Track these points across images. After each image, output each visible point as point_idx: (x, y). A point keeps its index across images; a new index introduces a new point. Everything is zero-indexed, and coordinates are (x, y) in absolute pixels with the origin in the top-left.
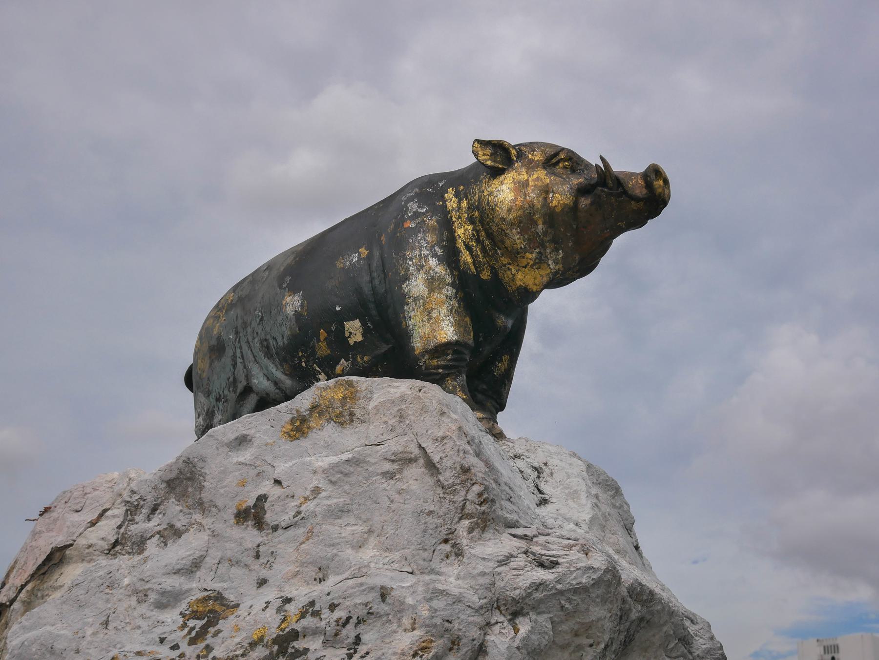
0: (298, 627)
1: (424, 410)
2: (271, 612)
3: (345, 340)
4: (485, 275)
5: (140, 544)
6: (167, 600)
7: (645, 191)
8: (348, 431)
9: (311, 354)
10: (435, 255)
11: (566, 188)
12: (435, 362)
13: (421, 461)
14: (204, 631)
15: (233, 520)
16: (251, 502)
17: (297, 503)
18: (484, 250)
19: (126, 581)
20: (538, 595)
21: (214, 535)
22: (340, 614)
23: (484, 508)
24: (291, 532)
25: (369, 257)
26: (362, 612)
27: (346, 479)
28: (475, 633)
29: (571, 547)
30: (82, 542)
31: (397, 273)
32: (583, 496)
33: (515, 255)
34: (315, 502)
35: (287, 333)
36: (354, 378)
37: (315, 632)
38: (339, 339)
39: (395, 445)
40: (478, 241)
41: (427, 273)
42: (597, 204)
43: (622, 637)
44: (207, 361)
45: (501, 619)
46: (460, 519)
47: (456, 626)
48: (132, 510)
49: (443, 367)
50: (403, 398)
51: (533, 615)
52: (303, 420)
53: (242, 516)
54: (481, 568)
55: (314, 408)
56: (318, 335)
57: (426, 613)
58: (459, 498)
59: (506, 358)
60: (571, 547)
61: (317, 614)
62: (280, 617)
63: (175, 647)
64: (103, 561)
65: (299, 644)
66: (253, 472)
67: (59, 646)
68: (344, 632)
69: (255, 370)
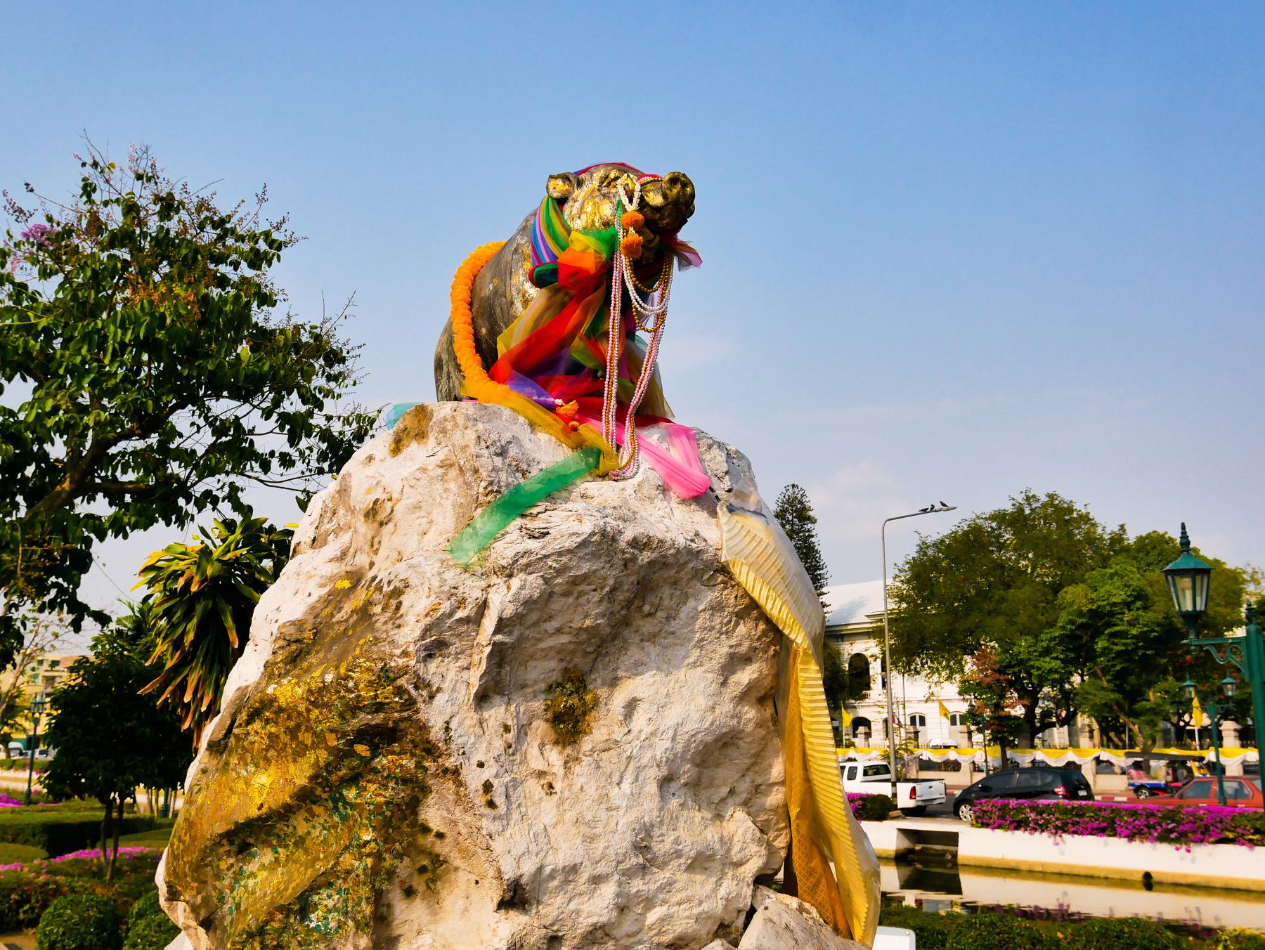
20: (524, 561)
23: (490, 498)
27: (419, 483)
28: (477, 593)
46: (476, 508)
47: (461, 591)
51: (522, 576)
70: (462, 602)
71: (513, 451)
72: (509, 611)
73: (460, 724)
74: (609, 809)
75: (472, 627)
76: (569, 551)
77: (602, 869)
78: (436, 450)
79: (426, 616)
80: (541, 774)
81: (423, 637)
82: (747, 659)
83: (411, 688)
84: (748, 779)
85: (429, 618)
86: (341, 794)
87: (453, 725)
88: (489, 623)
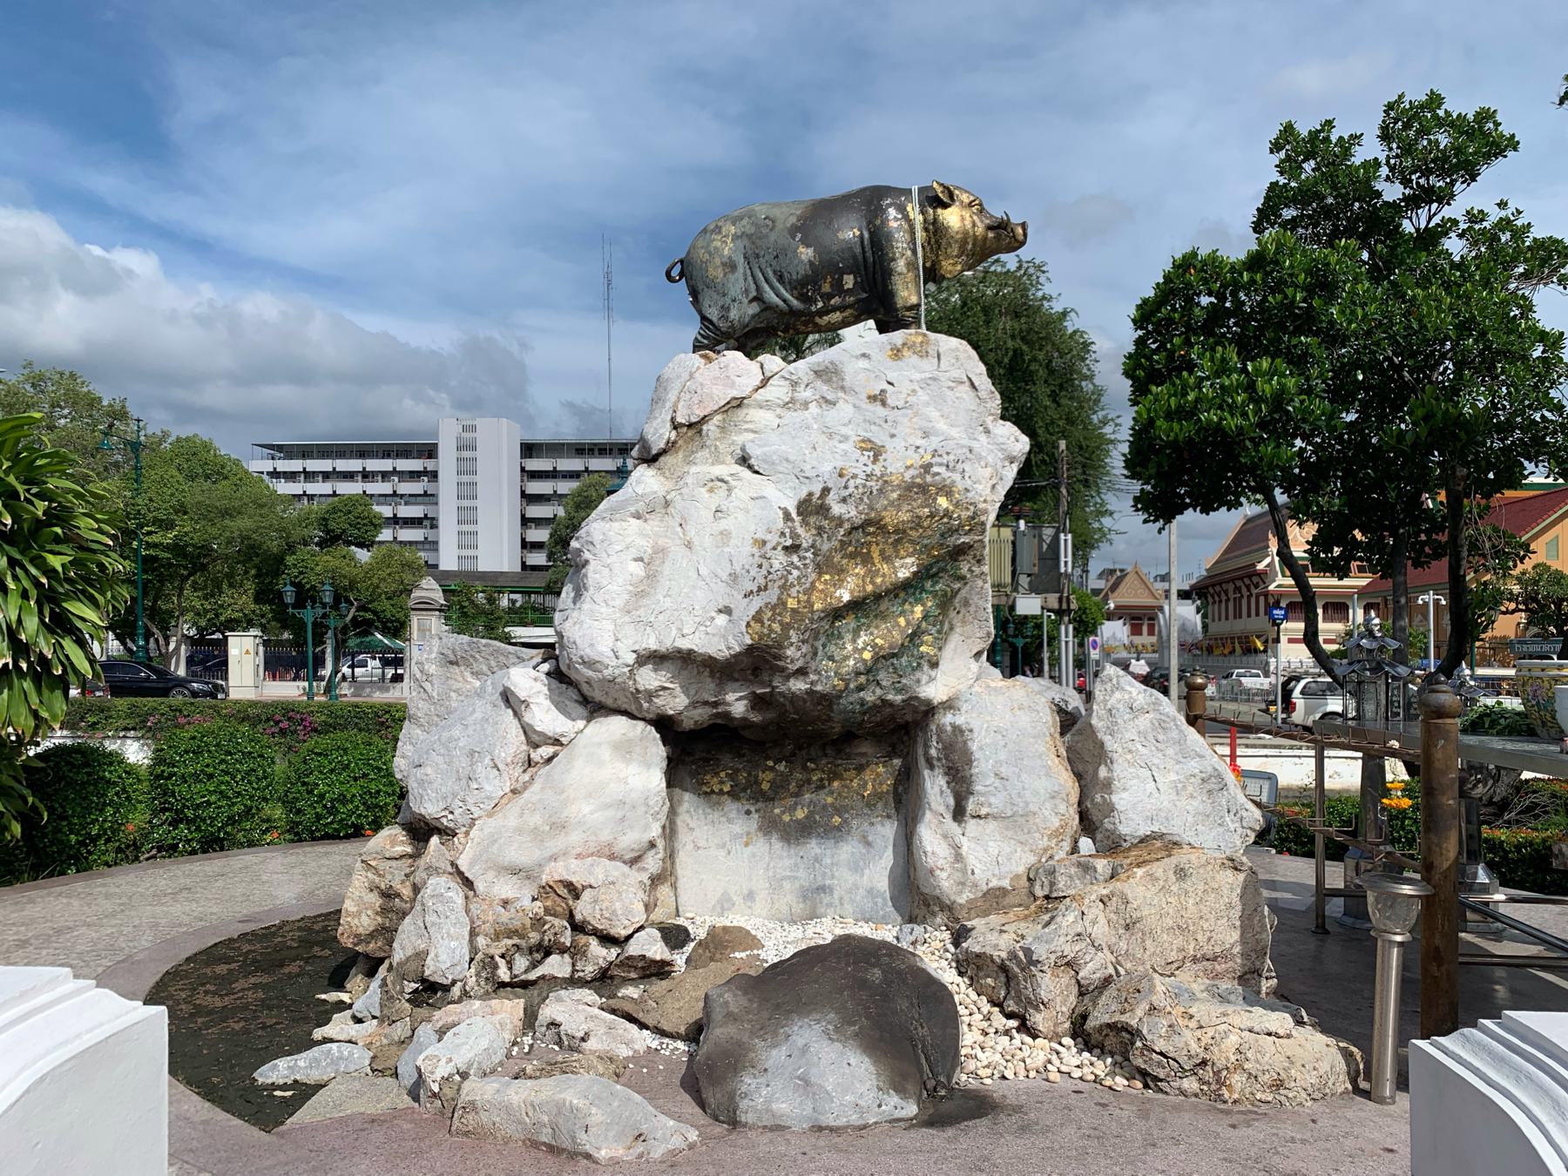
6: (845, 438)
8: (925, 360)
9: (818, 289)
12: (908, 313)
13: (968, 383)
19: (815, 426)
21: (855, 406)
31: (887, 254)
37: (941, 465)
38: (838, 288)
40: (929, 243)
42: (997, 238)
50: (957, 349)
54: (1001, 440)
55: (904, 344)
56: (825, 279)
61: (940, 456)
65: (935, 469)
67: (792, 458)
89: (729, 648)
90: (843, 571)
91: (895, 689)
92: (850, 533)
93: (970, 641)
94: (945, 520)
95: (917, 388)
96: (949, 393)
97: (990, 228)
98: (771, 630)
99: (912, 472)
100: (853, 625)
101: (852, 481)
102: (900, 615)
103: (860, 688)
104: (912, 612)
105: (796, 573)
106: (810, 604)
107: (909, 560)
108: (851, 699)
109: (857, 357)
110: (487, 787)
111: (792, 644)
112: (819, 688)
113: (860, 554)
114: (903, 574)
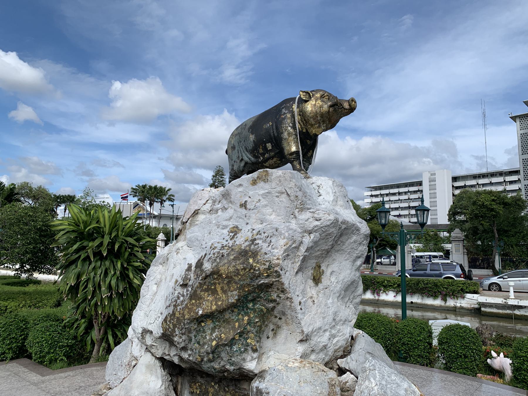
0: (256, 237)
1: (286, 180)
2: (249, 232)
3: (267, 149)
4: (304, 131)
5: (217, 211)
6: (225, 227)
7: (349, 107)
8: (267, 184)
10: (290, 126)
11: (326, 106)
12: (291, 157)
13: (286, 193)
14: (234, 236)
15: (239, 207)
16: (243, 202)
17: (255, 203)
18: (303, 124)
19: (214, 222)
20: (316, 229)
21: (235, 210)
22: (266, 234)
23: (302, 206)
24: (254, 211)
25: (272, 125)
26: (271, 234)
28: (300, 239)
29: (325, 214)
30: (202, 209)
31: (280, 131)
32: (331, 193)
33: (312, 125)
34: (259, 203)
35: (252, 146)
36: (268, 169)
37: (260, 239)
38: (265, 148)
39: (279, 189)
40: (302, 121)
41: (288, 132)
42: (335, 110)
43: (339, 234)
44: (231, 151)
45: (307, 235)
48: (214, 202)
49: (293, 158)
51: (314, 233)
52: (255, 181)
53: (241, 206)
54: (301, 222)
55: (258, 177)
57: (287, 235)
58: (295, 204)
59: (311, 151)
60: (325, 214)
61: (260, 234)
62: (252, 234)
63: (227, 241)
64: (208, 216)
65: (257, 242)
66: (243, 194)
67: (199, 239)
68: (267, 239)
69: (244, 155)
70: (294, 242)
71: (303, 189)
72: (311, 245)
73: (292, 282)
74: (328, 308)
75: (296, 249)
76: (328, 226)
77: (326, 327)
78: (276, 187)
79: (284, 246)
80: (311, 297)
81: (283, 253)
82: (359, 257)
83: (280, 270)
84: (353, 294)
85: (285, 247)
86: (247, 305)
87: (291, 283)
88: (303, 249)
89: (158, 334)
90: (201, 298)
91: (230, 363)
92: (205, 279)
93: (295, 334)
94: (252, 271)
95: (261, 198)
96: (277, 199)
97: (331, 106)
98: (169, 327)
99: (247, 243)
100: (212, 325)
101: (212, 251)
102: (237, 321)
103: (210, 361)
104: (243, 320)
105: (182, 298)
106: (184, 316)
107: (235, 293)
108: (207, 366)
109: (237, 186)
110: (119, 374)
111: (176, 335)
112: (191, 358)
113: (211, 289)
114: (232, 300)
